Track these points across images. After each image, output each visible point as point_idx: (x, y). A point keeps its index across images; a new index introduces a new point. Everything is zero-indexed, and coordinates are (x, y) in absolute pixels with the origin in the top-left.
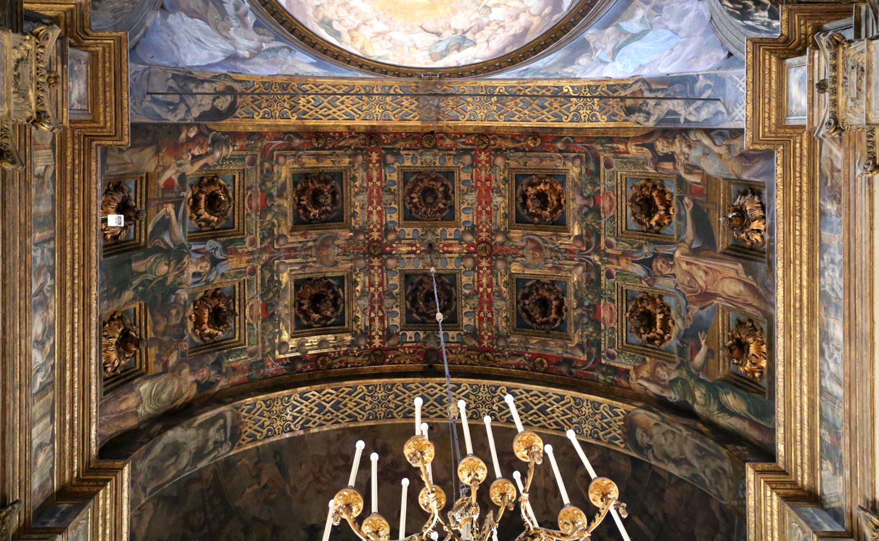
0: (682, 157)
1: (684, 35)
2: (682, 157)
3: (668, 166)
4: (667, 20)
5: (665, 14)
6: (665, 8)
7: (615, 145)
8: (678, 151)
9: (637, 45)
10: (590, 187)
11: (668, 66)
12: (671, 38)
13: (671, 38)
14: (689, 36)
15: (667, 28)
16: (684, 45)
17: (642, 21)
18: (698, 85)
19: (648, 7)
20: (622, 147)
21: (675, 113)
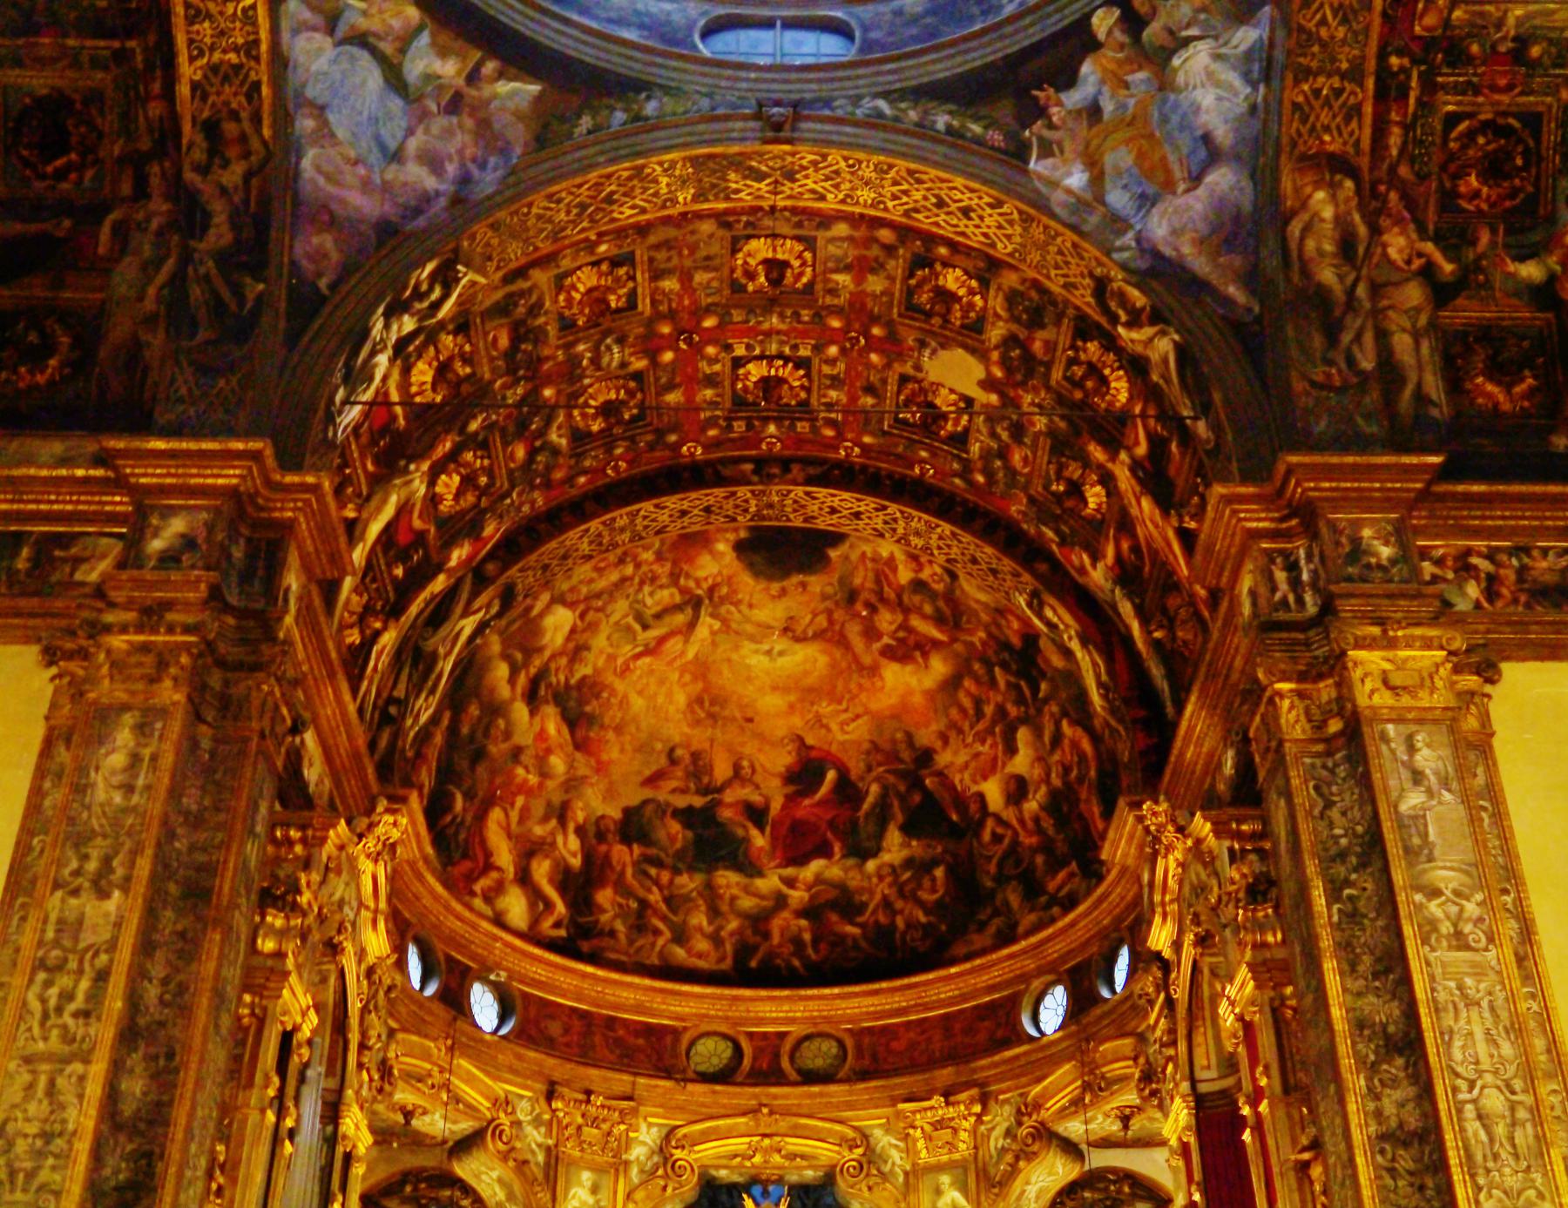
0: (140, 216)
1: (389, 176)
2: (140, 216)
3: (126, 189)
4: (427, 131)
5: (440, 123)
6: (454, 120)
7: (158, 73)
8: (152, 206)
9: (373, 78)
10: (72, 15)
11: (319, 169)
12: (383, 148)
13: (383, 148)
14: (386, 188)
15: (410, 132)
16: (366, 185)
17: (429, 77)
18: (248, 280)
19: (461, 82)
20: (157, 87)
21: (205, 228)
